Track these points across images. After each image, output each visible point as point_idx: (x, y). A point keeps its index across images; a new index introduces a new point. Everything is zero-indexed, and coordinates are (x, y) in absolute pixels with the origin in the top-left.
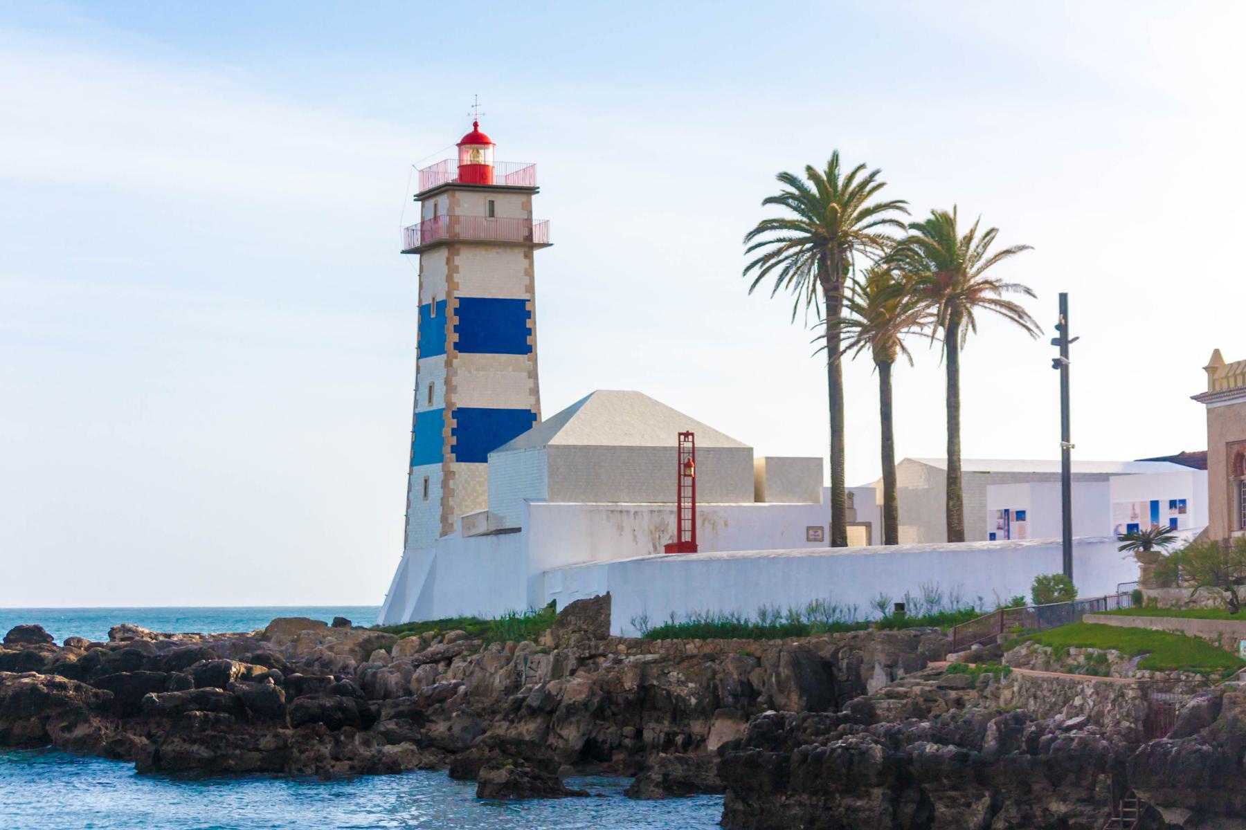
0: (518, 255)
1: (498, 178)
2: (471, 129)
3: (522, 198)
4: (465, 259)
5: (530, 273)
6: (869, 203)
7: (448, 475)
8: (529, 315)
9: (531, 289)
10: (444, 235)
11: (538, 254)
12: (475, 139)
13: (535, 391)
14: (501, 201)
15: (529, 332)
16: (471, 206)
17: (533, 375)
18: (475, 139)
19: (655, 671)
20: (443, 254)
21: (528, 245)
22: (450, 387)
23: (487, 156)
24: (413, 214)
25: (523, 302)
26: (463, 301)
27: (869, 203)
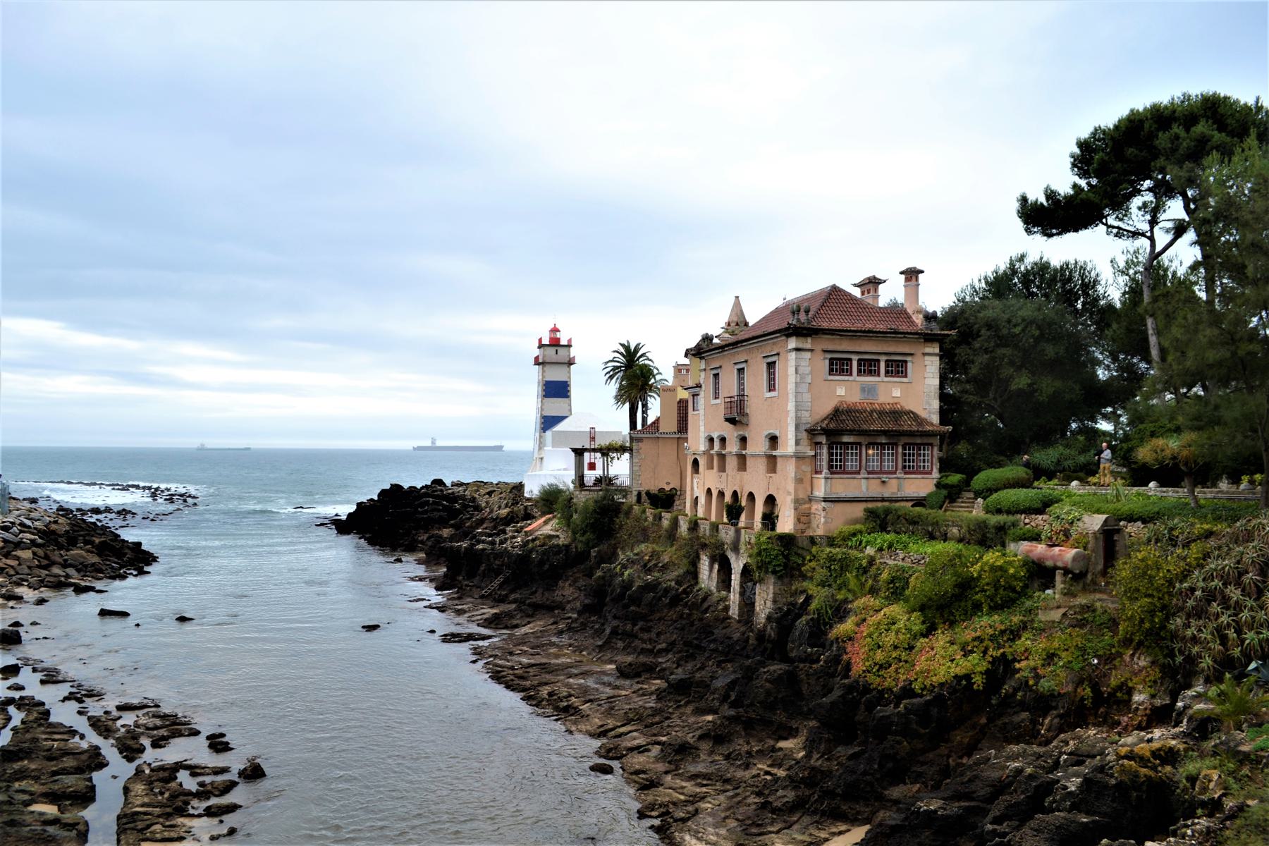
0: (566, 366)
1: (564, 342)
2: (553, 326)
3: (567, 349)
4: (547, 368)
5: (569, 372)
6: (638, 355)
7: (540, 437)
8: (568, 386)
9: (570, 377)
10: (541, 361)
11: (572, 367)
12: (555, 330)
13: (570, 410)
14: (561, 350)
15: (569, 391)
16: (552, 351)
17: (570, 405)
18: (555, 330)
19: (529, 508)
20: (541, 366)
21: (570, 363)
22: (542, 410)
23: (558, 335)
24: (537, 352)
25: (567, 382)
26: (546, 381)
27: (638, 355)
